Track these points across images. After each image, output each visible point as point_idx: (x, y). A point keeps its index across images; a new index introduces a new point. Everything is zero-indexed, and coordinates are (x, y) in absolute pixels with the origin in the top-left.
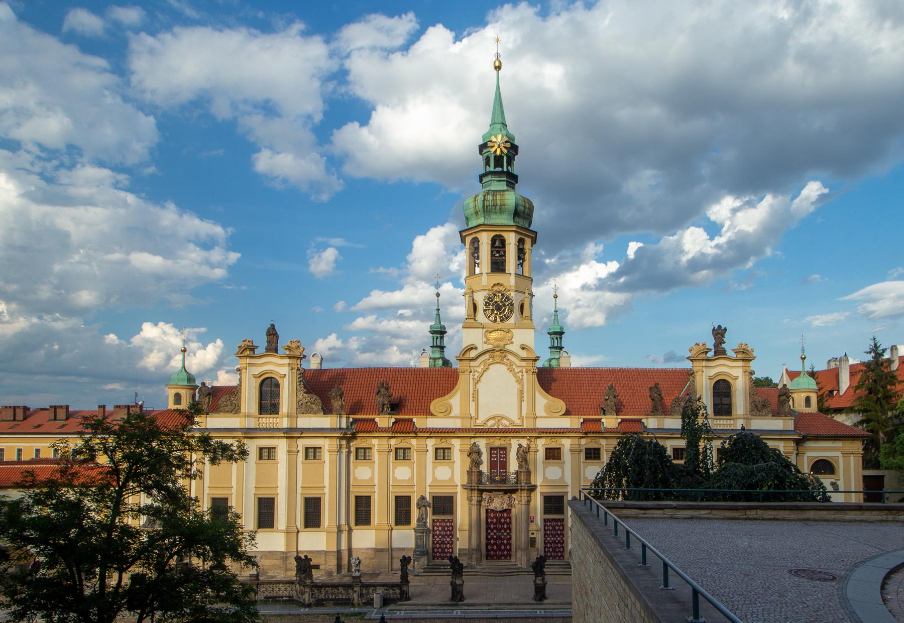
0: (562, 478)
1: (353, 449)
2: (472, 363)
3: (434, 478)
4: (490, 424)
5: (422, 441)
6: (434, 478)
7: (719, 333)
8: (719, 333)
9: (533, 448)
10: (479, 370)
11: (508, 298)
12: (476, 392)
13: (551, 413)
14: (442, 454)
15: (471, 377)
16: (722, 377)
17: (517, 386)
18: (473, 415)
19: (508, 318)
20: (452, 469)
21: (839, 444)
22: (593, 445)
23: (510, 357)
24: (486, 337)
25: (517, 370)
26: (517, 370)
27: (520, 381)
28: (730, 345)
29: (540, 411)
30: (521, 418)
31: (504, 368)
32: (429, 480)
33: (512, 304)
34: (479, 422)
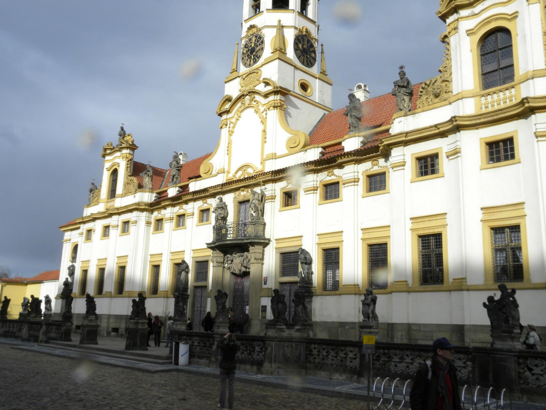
1: (153, 221)
2: (230, 116)
4: (239, 176)
9: (268, 193)
10: (233, 120)
13: (293, 148)
15: (228, 129)
18: (226, 169)
19: (259, 57)
23: (258, 97)
25: (262, 109)
26: (262, 109)
27: (263, 122)
29: (282, 149)
30: (263, 162)
34: (231, 176)
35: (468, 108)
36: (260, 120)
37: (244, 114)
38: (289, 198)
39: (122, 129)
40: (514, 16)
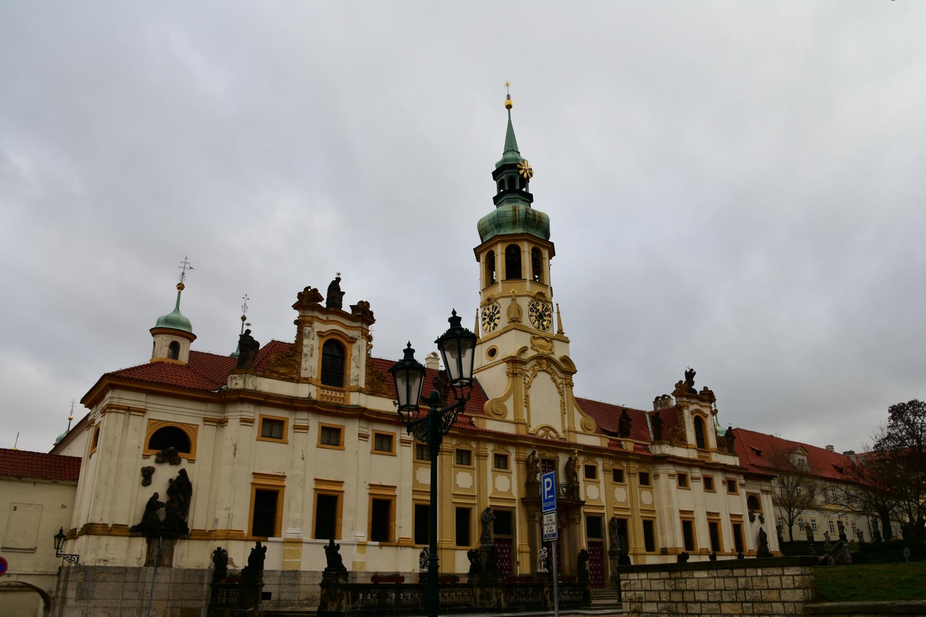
0: (599, 498)
2: (524, 367)
3: (495, 489)
4: (541, 432)
5: (481, 446)
6: (495, 489)
7: (690, 375)
8: (690, 375)
11: (547, 310)
12: (527, 396)
13: (586, 430)
14: (501, 462)
16: (698, 414)
17: (559, 397)
20: (510, 478)
21: (758, 483)
22: (618, 467)
24: (532, 342)
26: (559, 381)
27: (561, 393)
28: (698, 387)
31: (548, 377)
32: (490, 493)
33: (550, 316)
34: (531, 430)
35: (692, 454)
36: (556, 390)
37: (539, 374)
38: (591, 473)
39: (338, 279)
40: (706, 416)
